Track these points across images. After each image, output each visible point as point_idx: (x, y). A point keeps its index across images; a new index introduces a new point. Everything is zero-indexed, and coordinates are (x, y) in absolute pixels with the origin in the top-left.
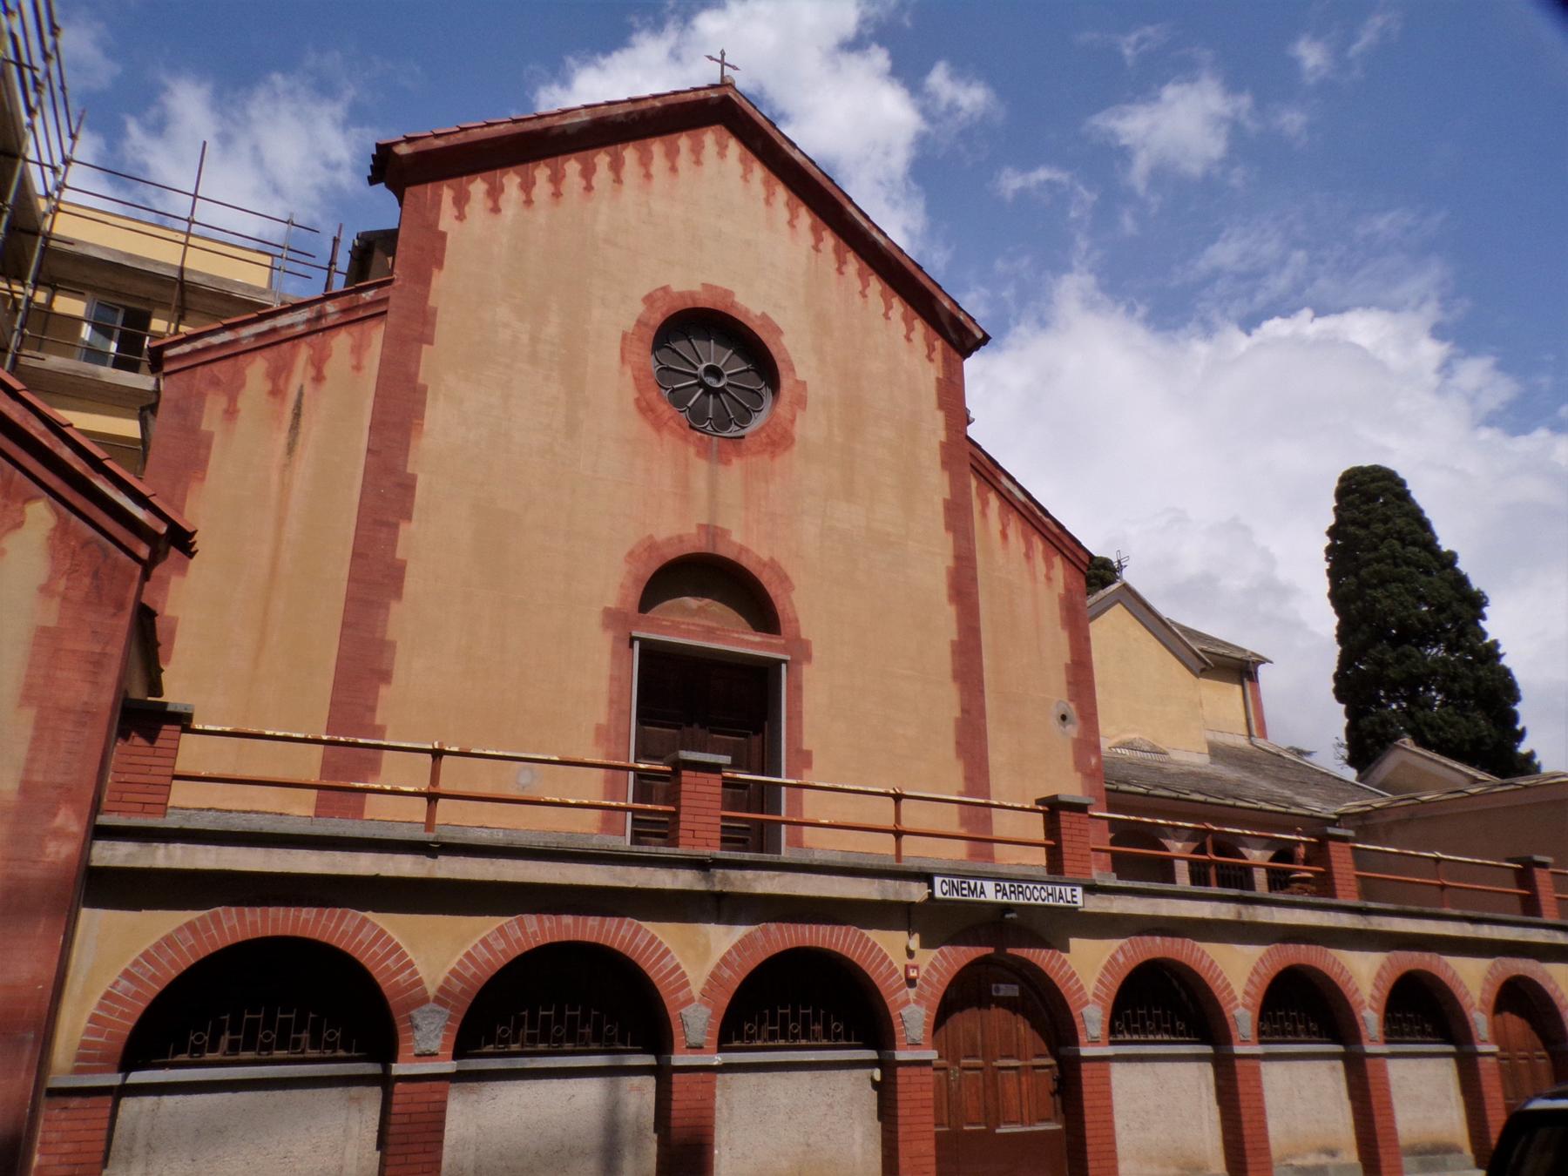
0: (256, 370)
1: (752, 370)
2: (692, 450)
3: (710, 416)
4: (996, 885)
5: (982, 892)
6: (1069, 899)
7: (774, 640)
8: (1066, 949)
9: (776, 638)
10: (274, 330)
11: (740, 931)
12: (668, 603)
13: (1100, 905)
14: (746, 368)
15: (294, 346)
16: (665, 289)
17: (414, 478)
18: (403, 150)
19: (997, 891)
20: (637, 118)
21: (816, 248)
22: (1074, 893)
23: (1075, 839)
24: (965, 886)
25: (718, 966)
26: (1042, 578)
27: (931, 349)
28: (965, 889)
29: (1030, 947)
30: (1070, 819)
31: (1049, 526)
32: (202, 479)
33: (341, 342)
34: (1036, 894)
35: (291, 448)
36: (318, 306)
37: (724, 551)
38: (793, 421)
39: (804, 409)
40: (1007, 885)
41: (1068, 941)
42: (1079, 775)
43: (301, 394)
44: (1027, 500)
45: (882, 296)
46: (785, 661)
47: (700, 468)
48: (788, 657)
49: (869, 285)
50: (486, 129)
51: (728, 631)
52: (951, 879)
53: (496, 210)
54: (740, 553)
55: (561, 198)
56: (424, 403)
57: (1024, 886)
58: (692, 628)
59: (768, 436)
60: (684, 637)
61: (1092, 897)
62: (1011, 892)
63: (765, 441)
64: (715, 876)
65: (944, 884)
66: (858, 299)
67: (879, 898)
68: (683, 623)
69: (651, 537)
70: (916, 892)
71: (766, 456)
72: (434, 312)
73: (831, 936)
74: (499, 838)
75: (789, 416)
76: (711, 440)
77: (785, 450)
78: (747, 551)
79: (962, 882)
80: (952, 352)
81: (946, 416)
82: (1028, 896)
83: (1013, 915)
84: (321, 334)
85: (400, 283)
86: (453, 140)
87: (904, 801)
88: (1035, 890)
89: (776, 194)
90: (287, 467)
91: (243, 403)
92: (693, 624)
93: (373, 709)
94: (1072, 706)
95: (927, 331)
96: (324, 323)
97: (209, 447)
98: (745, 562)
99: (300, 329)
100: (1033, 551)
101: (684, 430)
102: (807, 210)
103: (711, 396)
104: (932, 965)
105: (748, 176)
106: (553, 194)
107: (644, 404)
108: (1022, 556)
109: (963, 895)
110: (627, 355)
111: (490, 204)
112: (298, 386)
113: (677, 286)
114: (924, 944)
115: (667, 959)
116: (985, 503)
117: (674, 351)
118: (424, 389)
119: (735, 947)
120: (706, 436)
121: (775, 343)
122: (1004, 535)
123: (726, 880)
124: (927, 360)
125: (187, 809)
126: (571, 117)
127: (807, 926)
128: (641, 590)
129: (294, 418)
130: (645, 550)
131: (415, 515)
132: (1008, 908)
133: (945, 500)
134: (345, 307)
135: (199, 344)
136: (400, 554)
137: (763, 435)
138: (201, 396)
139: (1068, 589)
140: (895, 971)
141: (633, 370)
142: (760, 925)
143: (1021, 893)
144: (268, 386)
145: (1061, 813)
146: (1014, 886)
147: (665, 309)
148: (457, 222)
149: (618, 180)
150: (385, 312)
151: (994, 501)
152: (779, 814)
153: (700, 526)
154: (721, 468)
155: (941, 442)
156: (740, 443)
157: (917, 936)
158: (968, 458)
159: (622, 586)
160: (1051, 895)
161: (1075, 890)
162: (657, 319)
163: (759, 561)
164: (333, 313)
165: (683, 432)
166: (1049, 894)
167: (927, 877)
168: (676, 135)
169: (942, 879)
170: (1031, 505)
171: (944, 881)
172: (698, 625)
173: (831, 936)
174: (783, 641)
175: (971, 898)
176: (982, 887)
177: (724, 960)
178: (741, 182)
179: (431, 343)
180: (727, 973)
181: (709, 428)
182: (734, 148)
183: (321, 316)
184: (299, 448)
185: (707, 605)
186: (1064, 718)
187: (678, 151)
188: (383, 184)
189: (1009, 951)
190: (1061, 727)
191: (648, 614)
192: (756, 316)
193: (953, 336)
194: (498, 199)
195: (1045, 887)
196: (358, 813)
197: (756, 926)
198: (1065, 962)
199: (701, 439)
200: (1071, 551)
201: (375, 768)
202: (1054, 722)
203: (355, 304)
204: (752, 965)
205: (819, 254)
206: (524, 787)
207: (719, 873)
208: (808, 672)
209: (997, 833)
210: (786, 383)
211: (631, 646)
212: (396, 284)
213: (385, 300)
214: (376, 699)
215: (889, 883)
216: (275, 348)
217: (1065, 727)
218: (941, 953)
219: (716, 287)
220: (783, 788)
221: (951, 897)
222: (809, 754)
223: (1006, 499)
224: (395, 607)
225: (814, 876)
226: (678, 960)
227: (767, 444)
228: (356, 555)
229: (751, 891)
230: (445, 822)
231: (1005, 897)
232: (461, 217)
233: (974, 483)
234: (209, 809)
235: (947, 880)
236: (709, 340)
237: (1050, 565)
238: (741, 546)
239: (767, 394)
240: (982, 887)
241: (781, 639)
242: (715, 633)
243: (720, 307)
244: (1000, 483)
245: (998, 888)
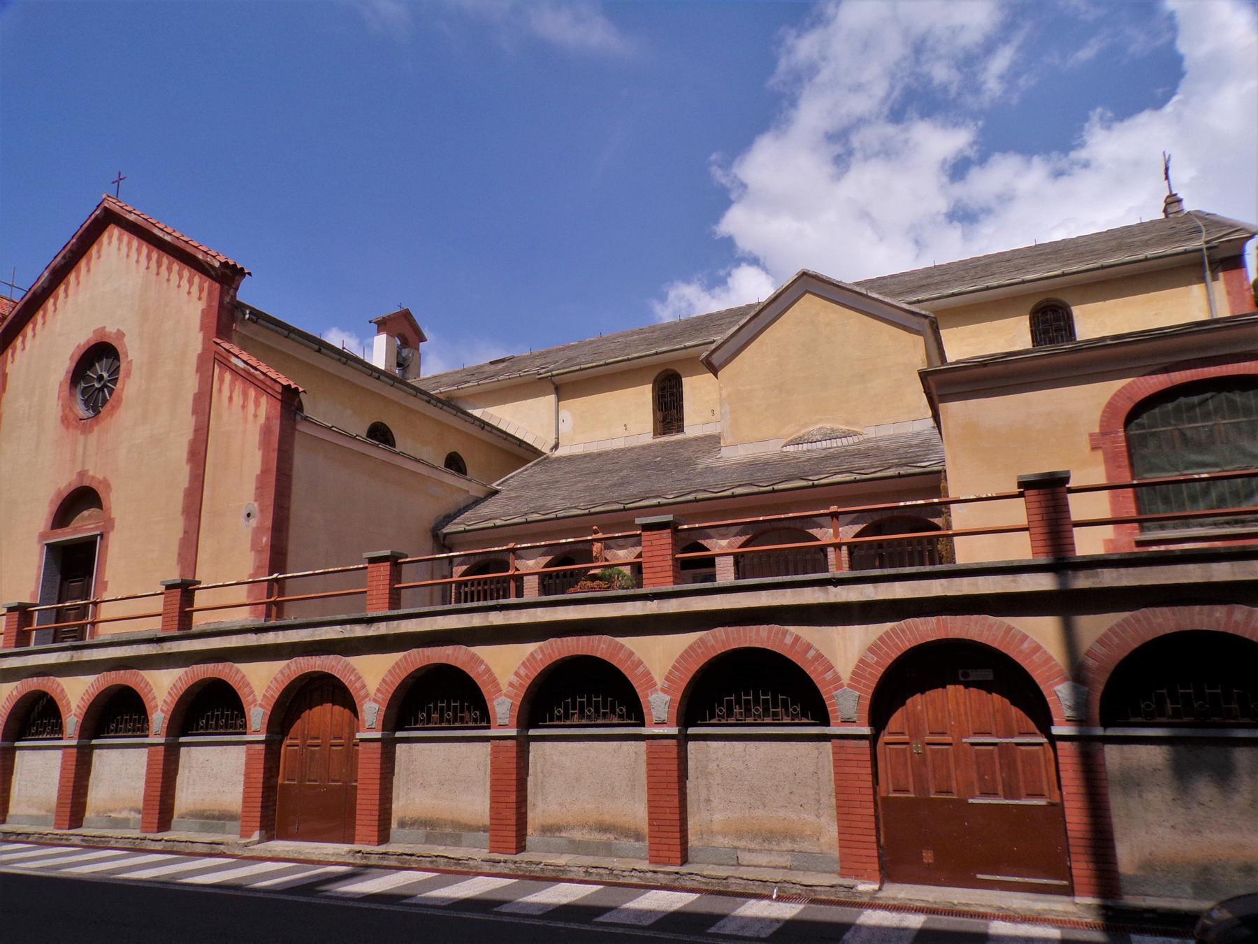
20: (70, 255)
26: (251, 418)
31: (258, 377)
66: (165, 285)
94: (256, 505)
108: (240, 407)
139: (268, 418)
151: (228, 376)
168: (89, 251)
186: (249, 515)
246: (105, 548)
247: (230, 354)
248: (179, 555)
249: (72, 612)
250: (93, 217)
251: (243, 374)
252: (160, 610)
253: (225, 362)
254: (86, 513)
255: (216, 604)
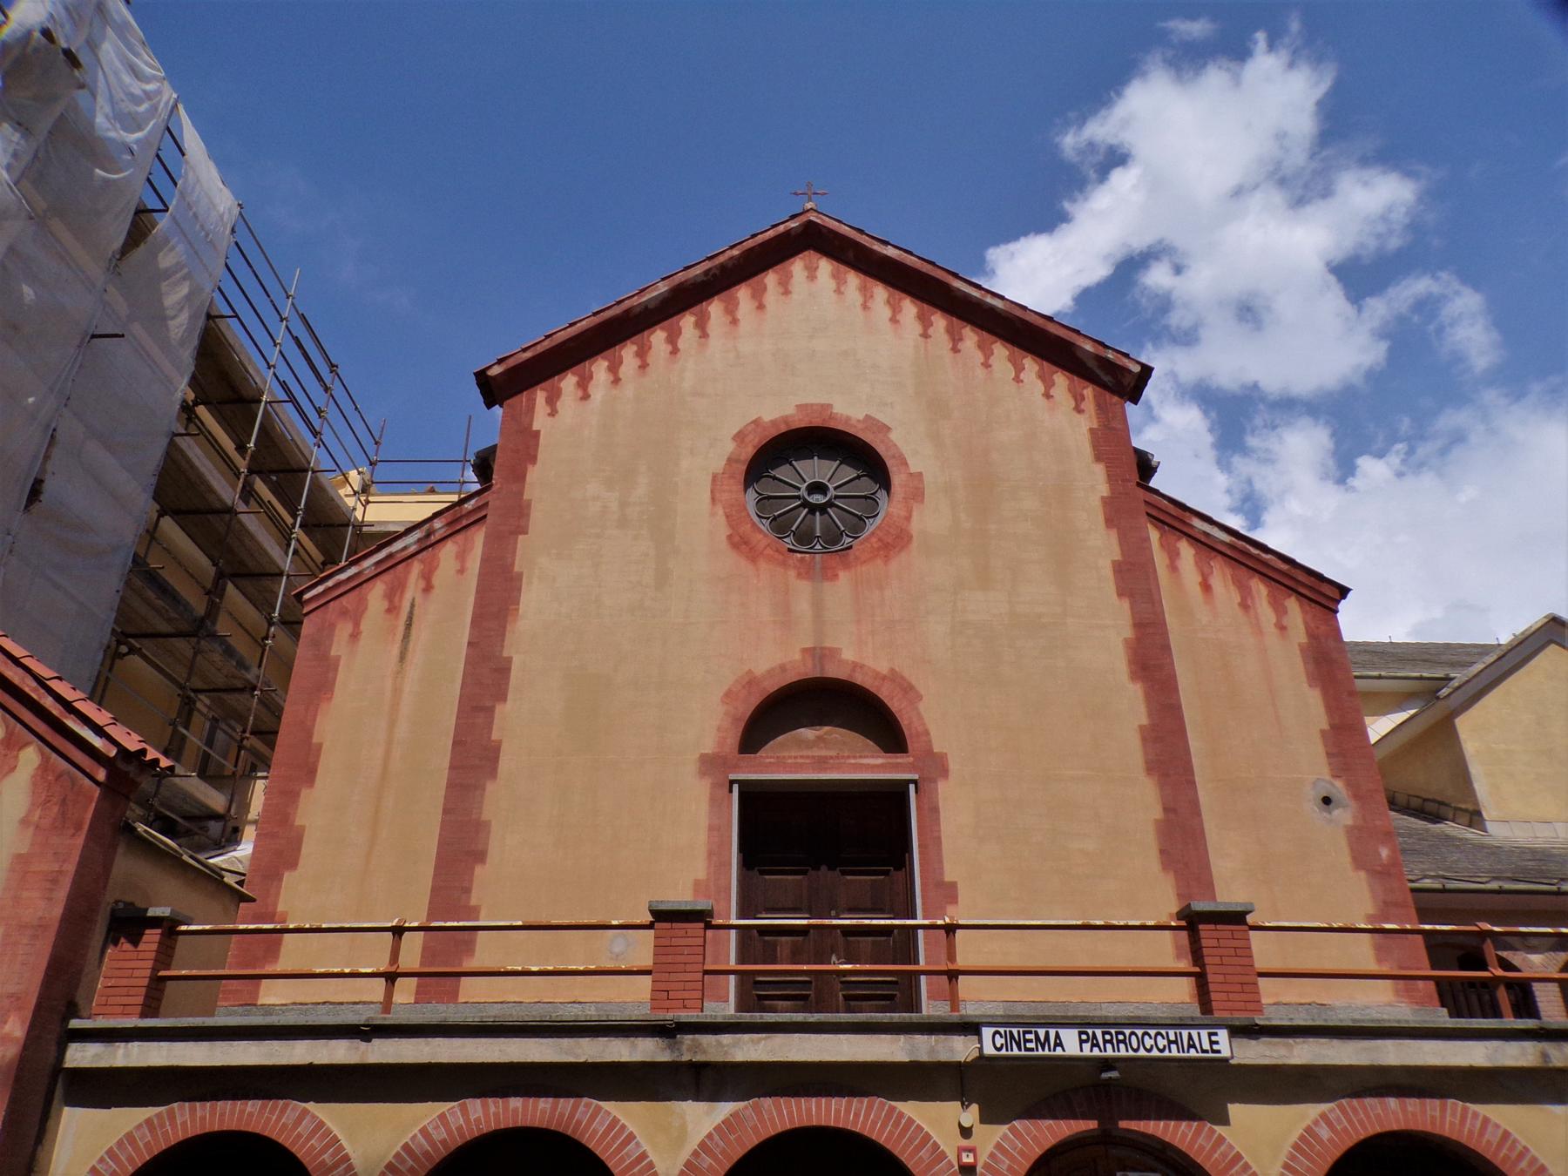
0: (376, 594)
1: (862, 476)
2: (792, 573)
3: (818, 535)
4: (1080, 1033)
5: (1059, 1044)
6: (1206, 1046)
7: (900, 759)
8: (1224, 1120)
9: (901, 757)
10: (390, 556)
11: (725, 1109)
12: (780, 738)
13: (1275, 1054)
14: (855, 475)
15: (408, 565)
16: (756, 422)
17: (509, 660)
18: (495, 371)
19: (1082, 1042)
20: (717, 272)
21: (925, 335)
22: (1214, 1038)
23: (1226, 960)
24: (1028, 1036)
25: (695, 1154)
27: (1079, 398)
28: (1031, 1041)
29: (1159, 1118)
30: (1215, 934)
31: (1272, 564)
32: (330, 699)
33: (448, 551)
34: (1148, 1042)
35: (402, 657)
36: (427, 526)
37: (833, 671)
38: (908, 518)
39: (922, 501)
40: (1099, 1032)
41: (1227, 1107)
42: (1363, 874)
43: (413, 606)
44: (1233, 539)
45: (1010, 360)
46: (915, 782)
47: (802, 591)
48: (916, 777)
49: (992, 354)
50: (569, 330)
51: (843, 757)
52: (1008, 1029)
53: (586, 397)
54: (853, 670)
55: (648, 369)
56: (519, 590)
57: (1127, 1032)
58: (799, 761)
59: (880, 540)
60: (791, 772)
61: (1253, 1042)
62: (1105, 1042)
63: (876, 546)
64: (682, 1043)
65: (997, 1036)
66: (980, 372)
67: (907, 1060)
68: (790, 757)
69: (750, 672)
70: (960, 1049)
71: (879, 562)
72: (529, 504)
73: (848, 1111)
74: (591, 1014)
75: (903, 513)
76: (814, 558)
77: (900, 551)
78: (862, 666)
79: (1025, 1033)
80: (1108, 395)
81: (1107, 467)
82: (1135, 1046)
83: (1114, 1074)
84: (430, 549)
85: (499, 486)
86: (539, 349)
87: (959, 932)
88: (1146, 1037)
89: (875, 295)
90: (399, 673)
91: (365, 625)
92: (802, 757)
93: (468, 891)
94: (1339, 784)
95: (1072, 381)
96: (433, 539)
97: (336, 670)
98: (859, 679)
99: (413, 549)
100: (1252, 598)
101: (783, 555)
102: (912, 301)
103: (818, 514)
104: (998, 1146)
105: (842, 289)
106: (640, 367)
107: (737, 539)
109: (1027, 1049)
110: (718, 495)
111: (580, 393)
112: (411, 599)
113: (768, 417)
114: (985, 1118)
115: (632, 1145)
116: (1174, 555)
117: (774, 478)
118: (520, 575)
119: (717, 1129)
120: (807, 555)
121: (882, 442)
122: (1206, 587)
123: (696, 1047)
124: (1075, 413)
125: (306, 1004)
126: (649, 293)
127: (814, 1099)
128: (741, 729)
129: (406, 629)
130: (744, 687)
131: (510, 696)
132: (1107, 1064)
133: (1114, 562)
134: (449, 520)
135: (330, 583)
136: (495, 736)
137: (874, 540)
138: (332, 626)
140: (943, 1156)
141: (724, 508)
142: (751, 1101)
143: (1124, 1042)
144: (385, 605)
145: (1201, 927)
146: (1110, 1034)
147: (756, 440)
148: (550, 419)
149: (704, 335)
150: (485, 516)
151: (1186, 551)
152: (916, 962)
153: (805, 651)
154: (827, 585)
155: (1103, 498)
156: (848, 554)
157: (975, 1108)
158: (1143, 507)
159: (719, 729)
160: (1175, 1042)
161: (1216, 1034)
162: (749, 451)
163: (877, 675)
164: (440, 528)
165: (781, 557)
166: (1170, 1042)
167: (971, 1028)
168: (763, 274)
169: (994, 1029)
170: (1241, 543)
171: (997, 1032)
172: (808, 757)
173: (848, 1111)
174: (911, 759)
175: (1040, 1052)
176: (1057, 1035)
177: (702, 1145)
178: (834, 296)
179: (526, 533)
180: (708, 1161)
181: (818, 547)
182: (825, 266)
183: (428, 535)
184: (409, 656)
185: (825, 734)
186: (1327, 801)
187: (765, 289)
188: (497, 406)
189: (1123, 1124)
190: (1325, 814)
191: (758, 754)
192: (859, 421)
193: (1107, 379)
194: (587, 387)
195: (1163, 1032)
196: (453, 996)
197: (746, 1102)
198: (1221, 1139)
199: (802, 560)
200: (1311, 588)
201: (469, 949)
202: (1312, 808)
203: (459, 515)
204: (739, 1152)
205: (929, 340)
206: (617, 956)
207: (688, 1039)
208: (946, 792)
209: (1261, 964)
210: (897, 480)
211: (731, 791)
212: (494, 489)
213: (486, 504)
214: (471, 881)
215: (920, 1039)
216: (392, 571)
217: (1330, 813)
218: (1014, 1131)
219: (812, 405)
220: (920, 932)
221: (1010, 1053)
222: (953, 886)
223: (1205, 545)
224: (490, 787)
225: (813, 1036)
226: (645, 1147)
227: (879, 549)
228: (455, 743)
229: (729, 1059)
230: (536, 1000)
231: (1095, 1049)
232: (553, 413)
233: (1154, 535)
234: (324, 1003)
235: (1002, 1030)
236: (813, 458)
237: (1280, 610)
238: (853, 662)
239: (882, 494)
240: (1057, 1035)
241: (909, 756)
242: (827, 763)
243: (817, 422)
244: (1192, 527)
245: (1084, 1037)
246: (932, 812)
247: (1188, 514)
248: (1162, 852)
249: (784, 939)
250: (782, 228)
251: (1228, 552)
252: (647, 961)
253: (1176, 524)
254: (808, 733)
255: (1098, 965)
